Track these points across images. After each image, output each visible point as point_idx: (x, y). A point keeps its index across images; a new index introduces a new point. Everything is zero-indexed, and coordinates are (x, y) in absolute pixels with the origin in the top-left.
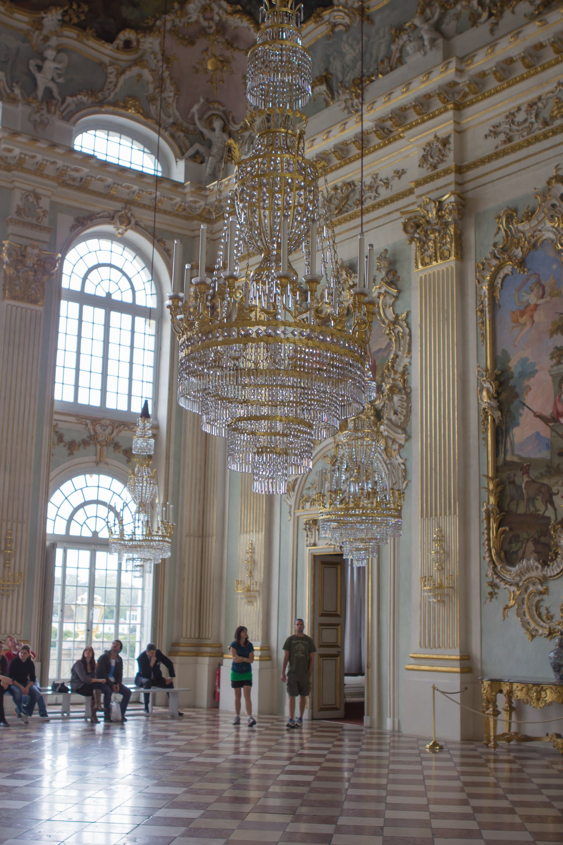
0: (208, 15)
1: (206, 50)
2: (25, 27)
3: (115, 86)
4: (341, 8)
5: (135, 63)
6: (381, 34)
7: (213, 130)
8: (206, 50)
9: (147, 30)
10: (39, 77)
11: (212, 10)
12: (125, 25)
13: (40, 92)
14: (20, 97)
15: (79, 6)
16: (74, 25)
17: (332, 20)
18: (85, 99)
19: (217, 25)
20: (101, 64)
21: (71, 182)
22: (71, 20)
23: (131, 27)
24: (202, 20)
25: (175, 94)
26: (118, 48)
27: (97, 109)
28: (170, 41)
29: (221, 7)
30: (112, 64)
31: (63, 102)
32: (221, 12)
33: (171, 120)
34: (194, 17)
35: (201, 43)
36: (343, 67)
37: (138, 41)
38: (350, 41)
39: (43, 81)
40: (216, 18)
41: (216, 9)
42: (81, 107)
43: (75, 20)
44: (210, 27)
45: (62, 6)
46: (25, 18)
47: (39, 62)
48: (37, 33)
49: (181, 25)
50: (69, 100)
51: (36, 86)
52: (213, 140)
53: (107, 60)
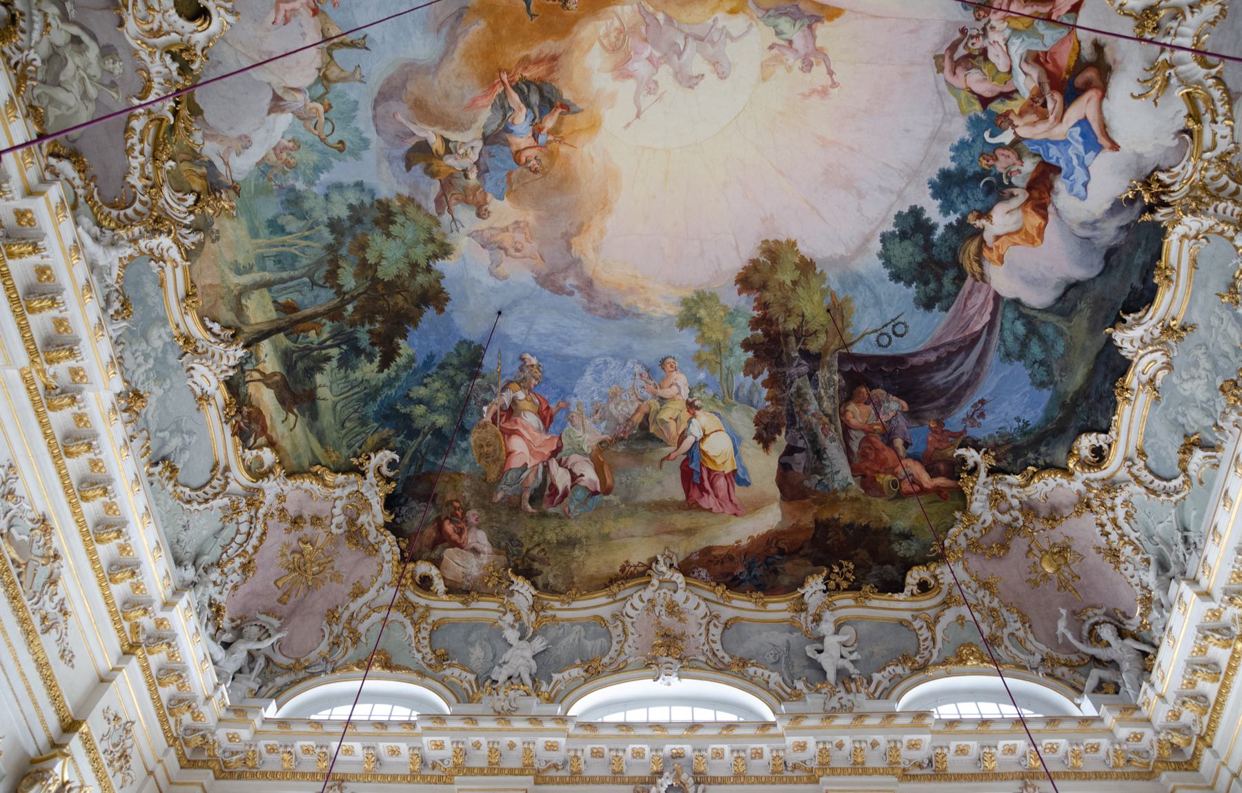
0: (1003, 506)
1: (1030, 550)
2: (787, 615)
3: (934, 640)
4: (1141, 352)
5: (945, 604)
6: (1215, 322)
7: (1108, 645)
8: (1030, 550)
9: (941, 558)
10: (821, 658)
11: (1003, 496)
12: (907, 565)
13: (831, 676)
14: (805, 690)
15: (841, 567)
16: (845, 590)
17: (1145, 378)
18: (899, 670)
19: (1021, 510)
20: (901, 622)
21: (917, 771)
22: (838, 586)
23: (918, 565)
24: (999, 516)
25: (1024, 624)
26: (912, 594)
27: (921, 676)
28: (974, 562)
29: (1011, 485)
30: (915, 618)
31: (870, 682)
32: (1015, 491)
33: (1038, 657)
34: (989, 519)
35: (1019, 544)
36: (1203, 409)
37: (935, 577)
38: (1185, 376)
39: (829, 662)
40: (1015, 502)
41: (1006, 490)
42: (896, 681)
43: (845, 585)
44: (1016, 519)
45: (819, 573)
46: (784, 606)
47: (819, 646)
48: (803, 615)
49: (978, 535)
50: (877, 677)
51: (825, 673)
52: (1114, 657)
53: (907, 616)
